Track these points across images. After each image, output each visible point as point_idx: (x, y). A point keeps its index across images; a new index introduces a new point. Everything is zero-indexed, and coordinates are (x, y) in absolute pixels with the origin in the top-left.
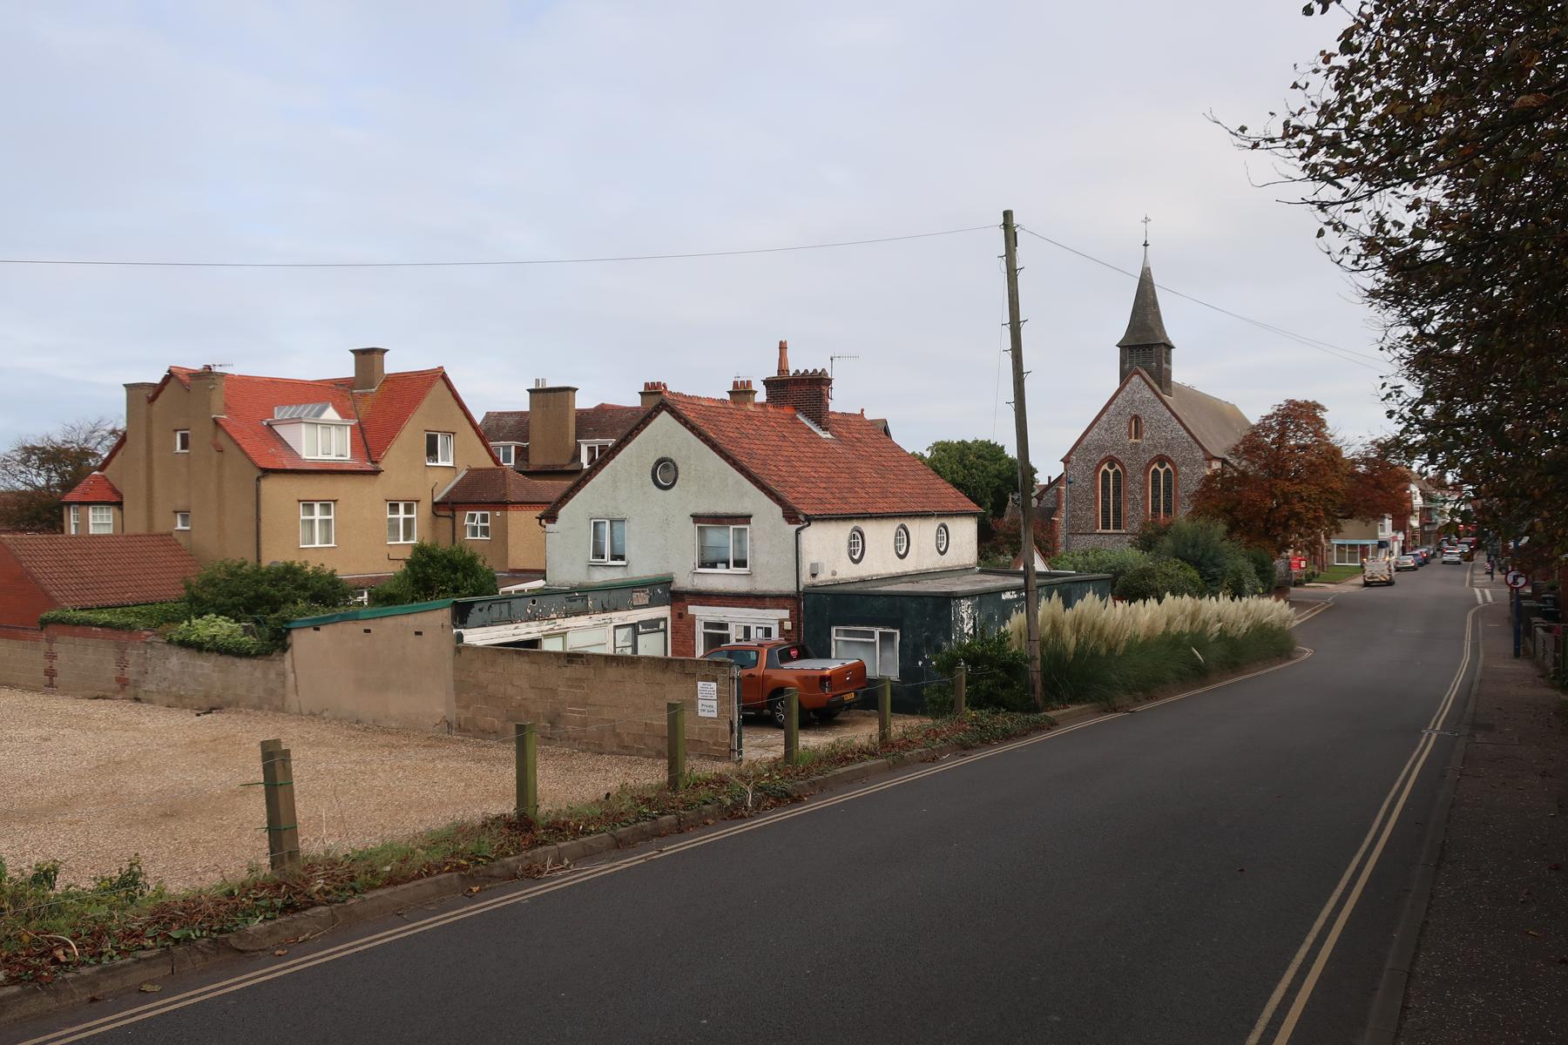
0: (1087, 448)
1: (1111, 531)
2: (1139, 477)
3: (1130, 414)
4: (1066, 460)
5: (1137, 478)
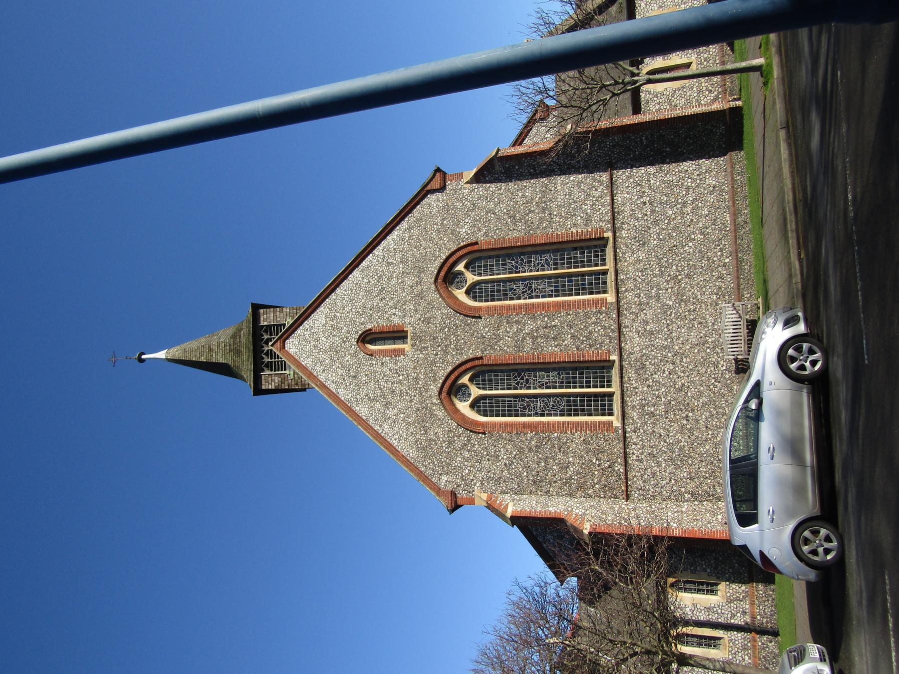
0: (424, 448)
1: (615, 388)
2: (483, 326)
3: (355, 355)
5: (487, 332)
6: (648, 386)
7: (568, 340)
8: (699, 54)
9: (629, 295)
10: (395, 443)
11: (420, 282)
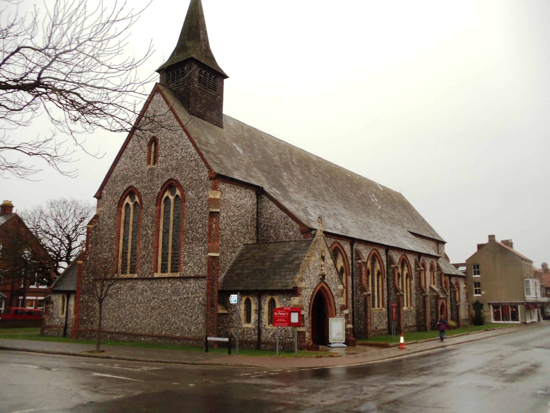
2: (152, 208)
4: (99, 196)
6: (126, 291)
7: (143, 253)
8: (254, 329)
9: (156, 284)
10: (118, 165)
11: (173, 170)
